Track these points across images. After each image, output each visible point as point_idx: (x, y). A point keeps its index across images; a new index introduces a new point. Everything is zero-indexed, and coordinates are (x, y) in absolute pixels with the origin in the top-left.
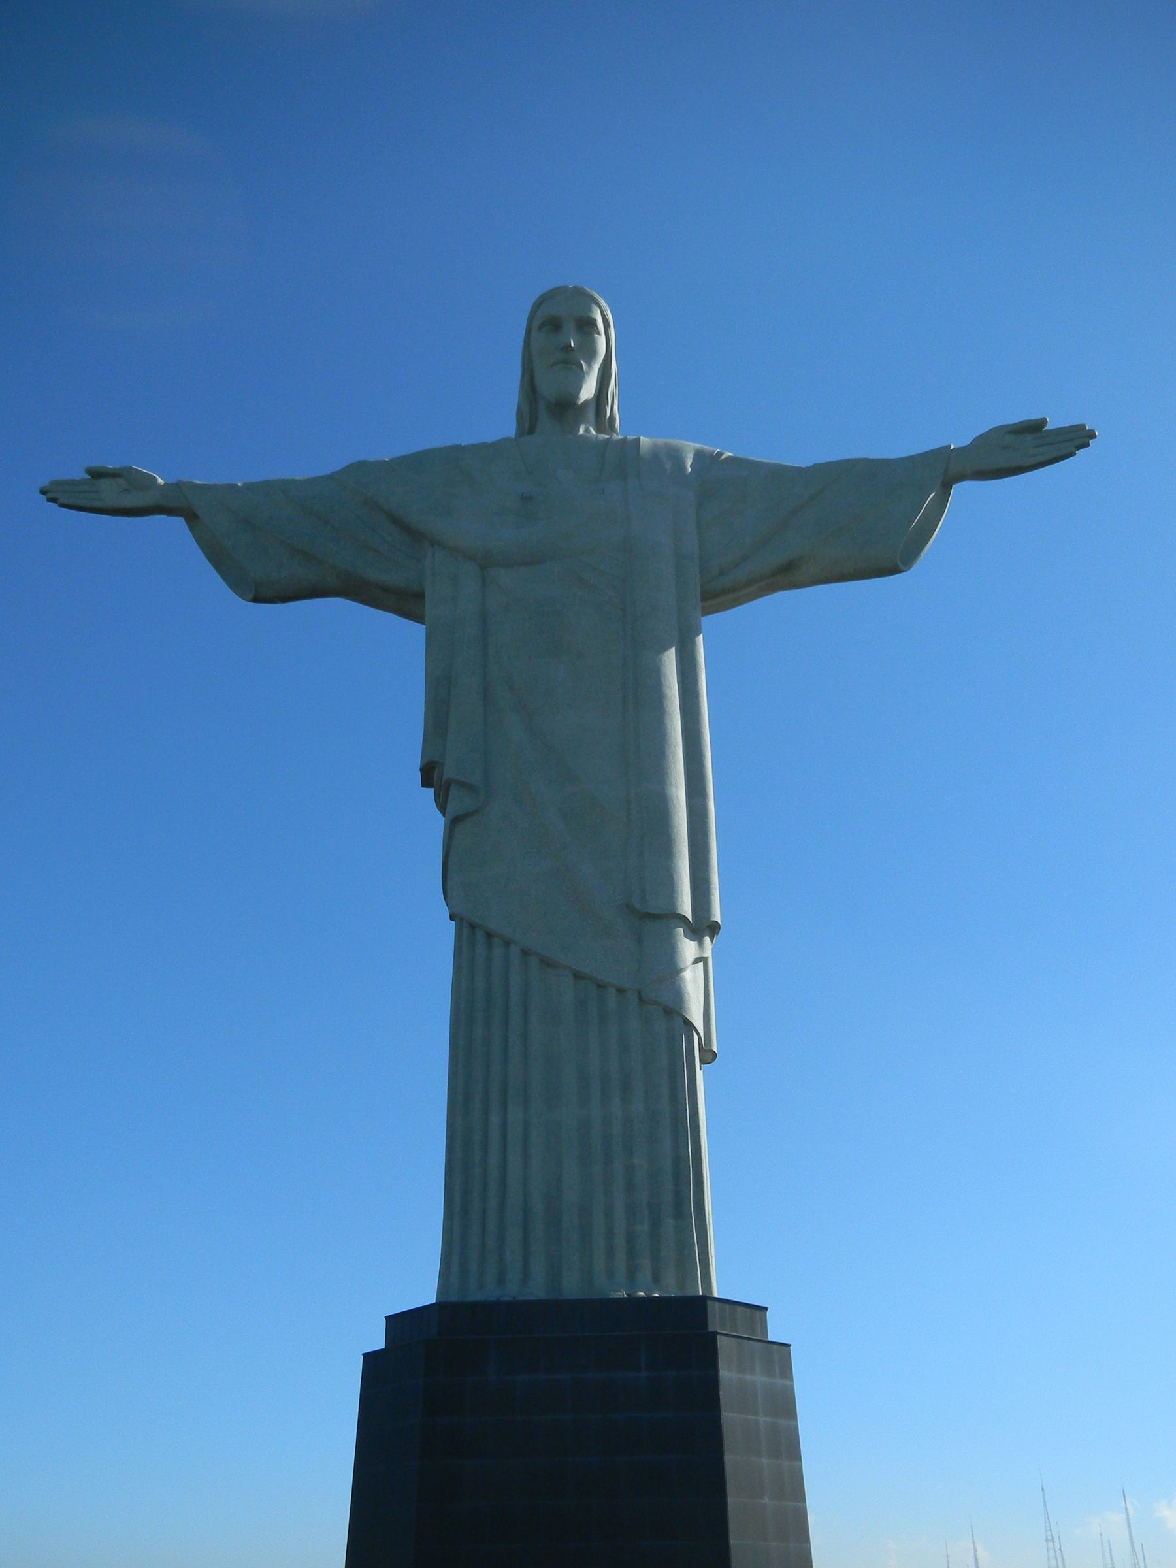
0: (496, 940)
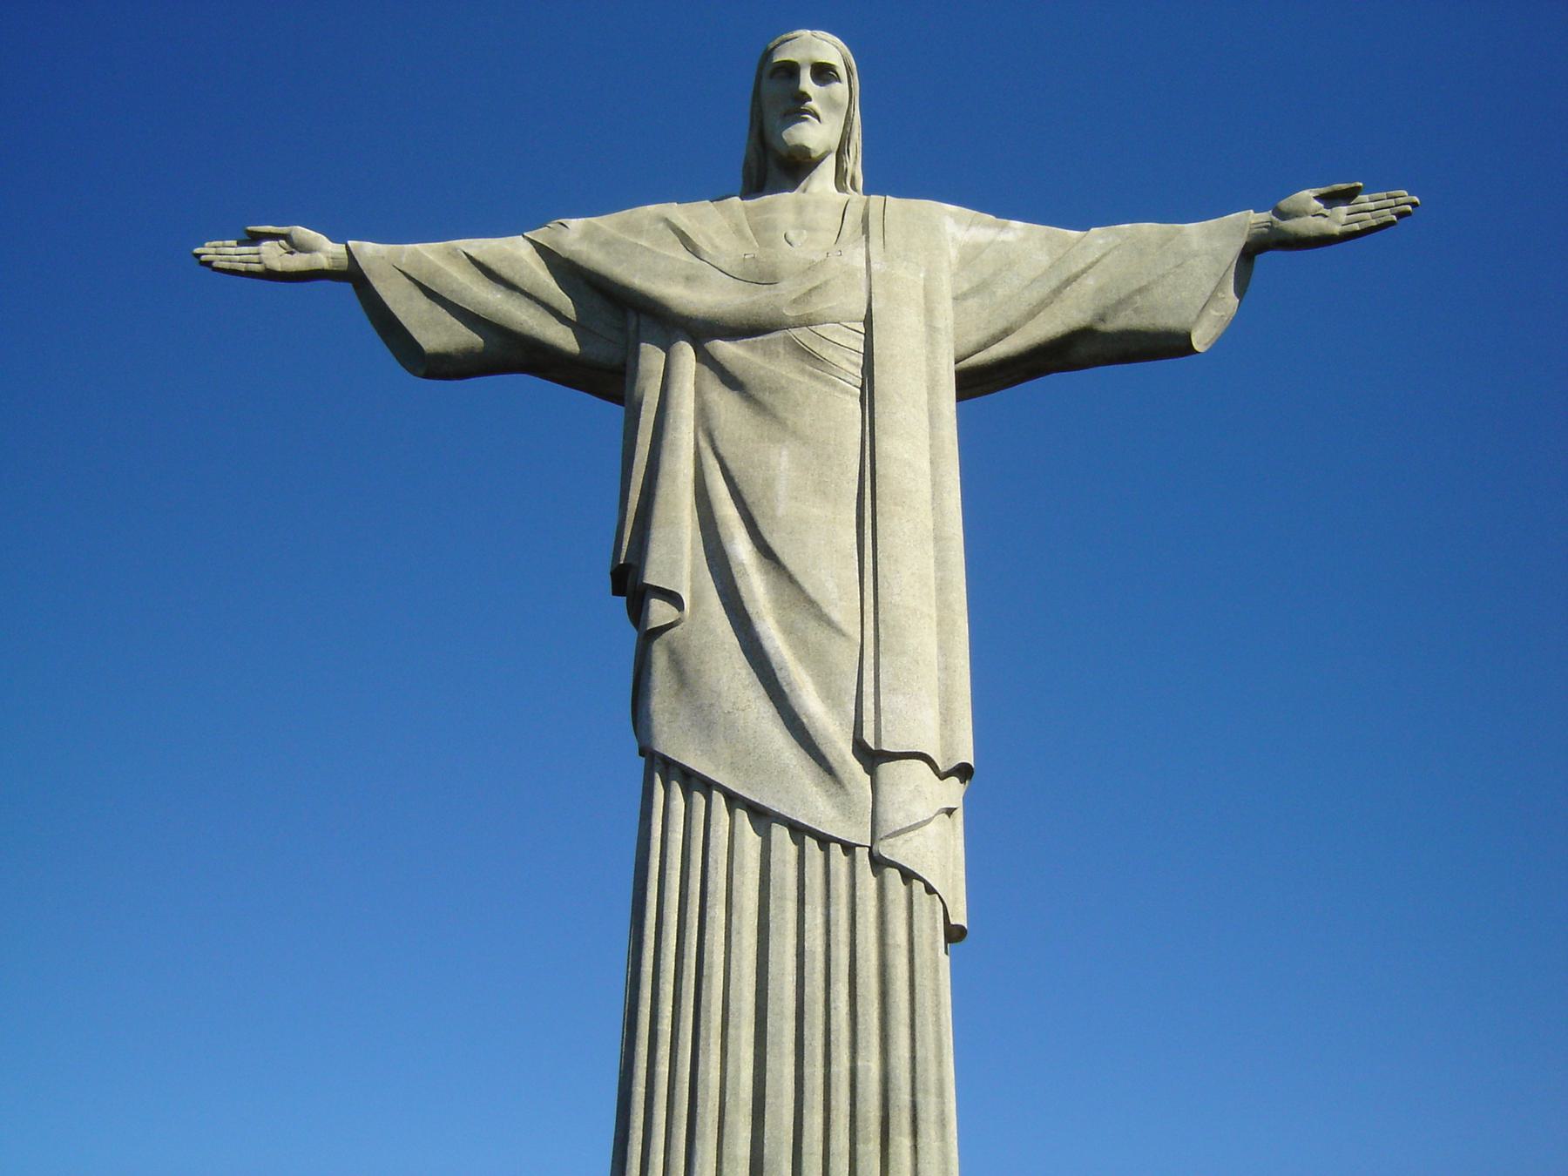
0: (694, 780)
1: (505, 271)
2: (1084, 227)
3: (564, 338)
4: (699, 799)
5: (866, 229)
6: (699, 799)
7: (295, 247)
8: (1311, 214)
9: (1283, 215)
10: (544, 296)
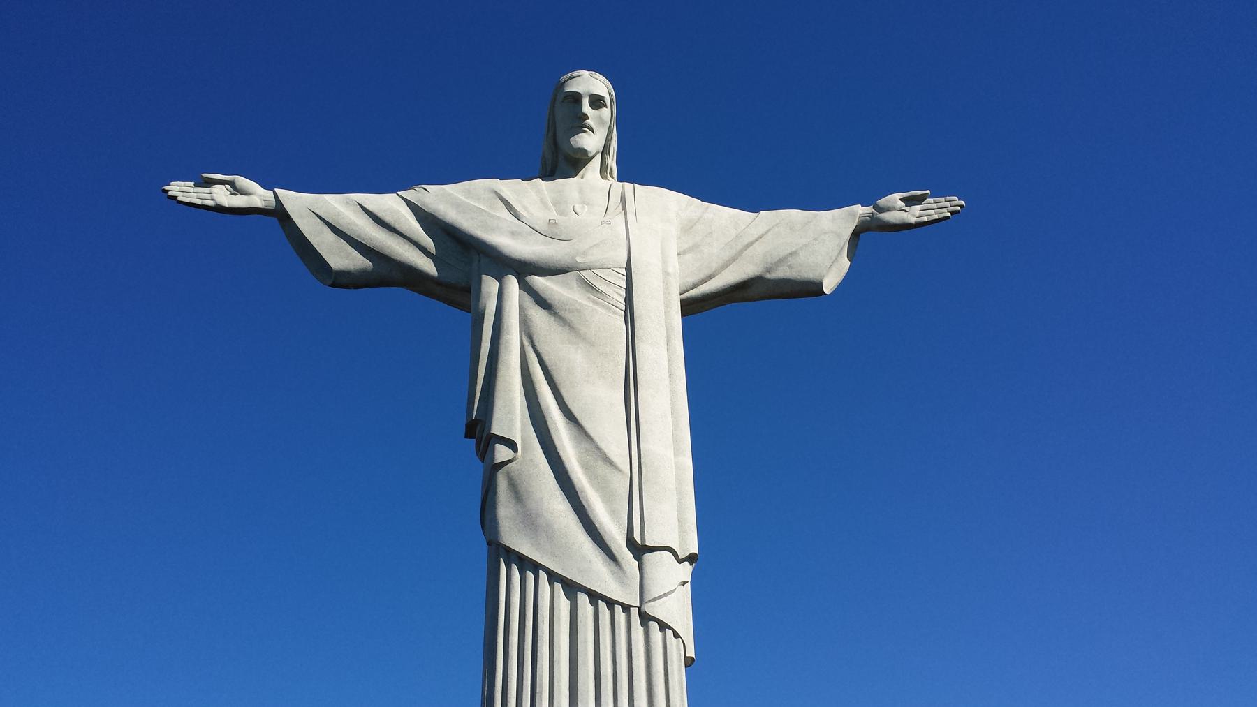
1: (388, 218)
2: (755, 209)
3: (428, 266)
4: (530, 576)
5: (624, 207)
6: (530, 576)
7: (236, 190)
8: (896, 208)
9: (881, 210)
10: (415, 238)
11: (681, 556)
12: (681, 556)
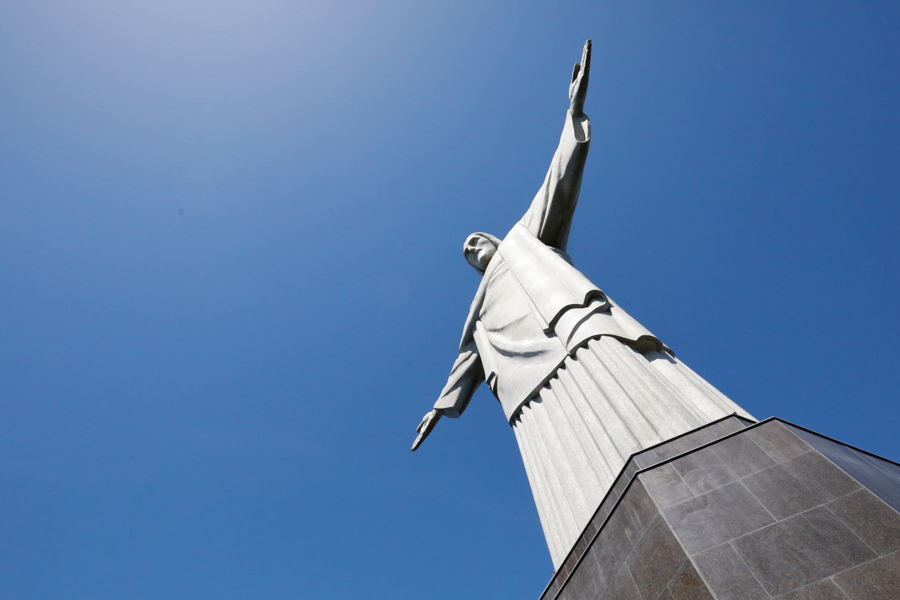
11: (582, 302)
12: (582, 302)
